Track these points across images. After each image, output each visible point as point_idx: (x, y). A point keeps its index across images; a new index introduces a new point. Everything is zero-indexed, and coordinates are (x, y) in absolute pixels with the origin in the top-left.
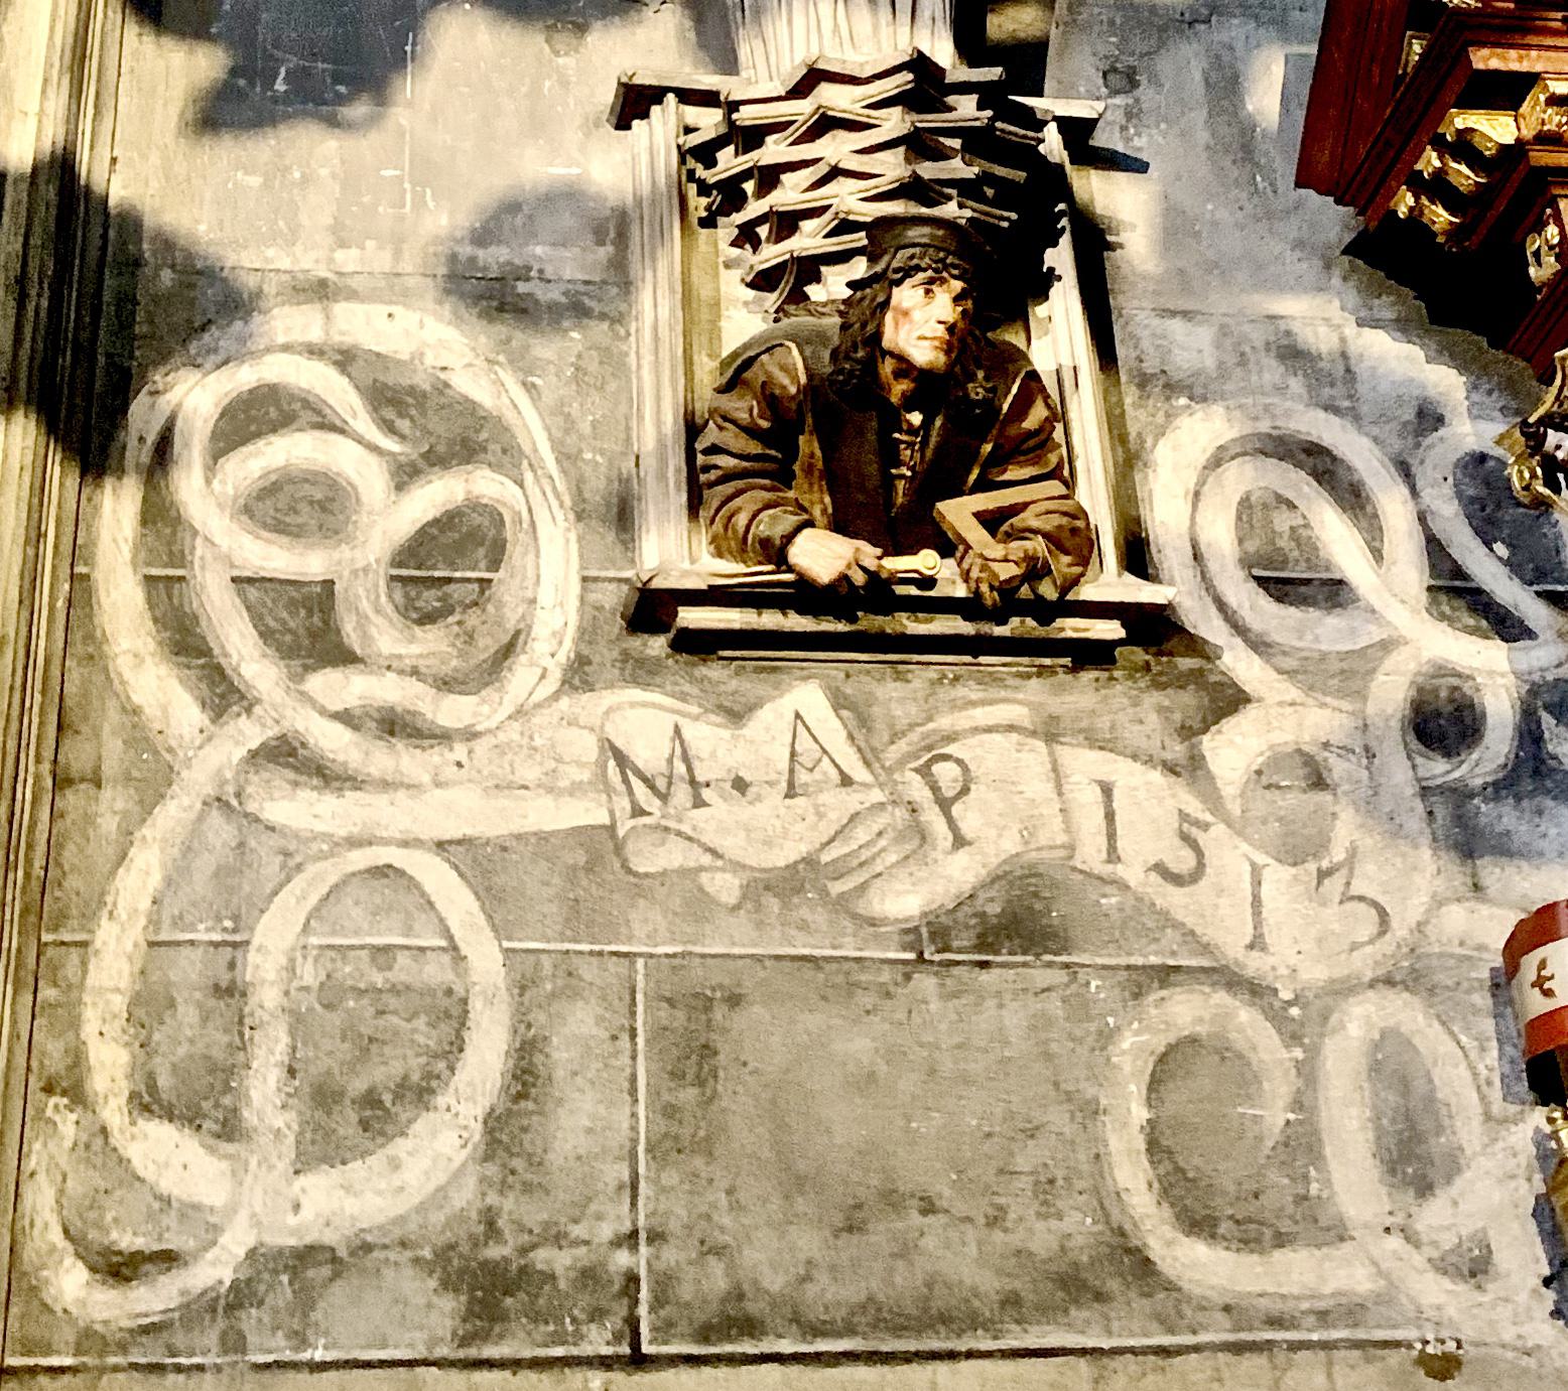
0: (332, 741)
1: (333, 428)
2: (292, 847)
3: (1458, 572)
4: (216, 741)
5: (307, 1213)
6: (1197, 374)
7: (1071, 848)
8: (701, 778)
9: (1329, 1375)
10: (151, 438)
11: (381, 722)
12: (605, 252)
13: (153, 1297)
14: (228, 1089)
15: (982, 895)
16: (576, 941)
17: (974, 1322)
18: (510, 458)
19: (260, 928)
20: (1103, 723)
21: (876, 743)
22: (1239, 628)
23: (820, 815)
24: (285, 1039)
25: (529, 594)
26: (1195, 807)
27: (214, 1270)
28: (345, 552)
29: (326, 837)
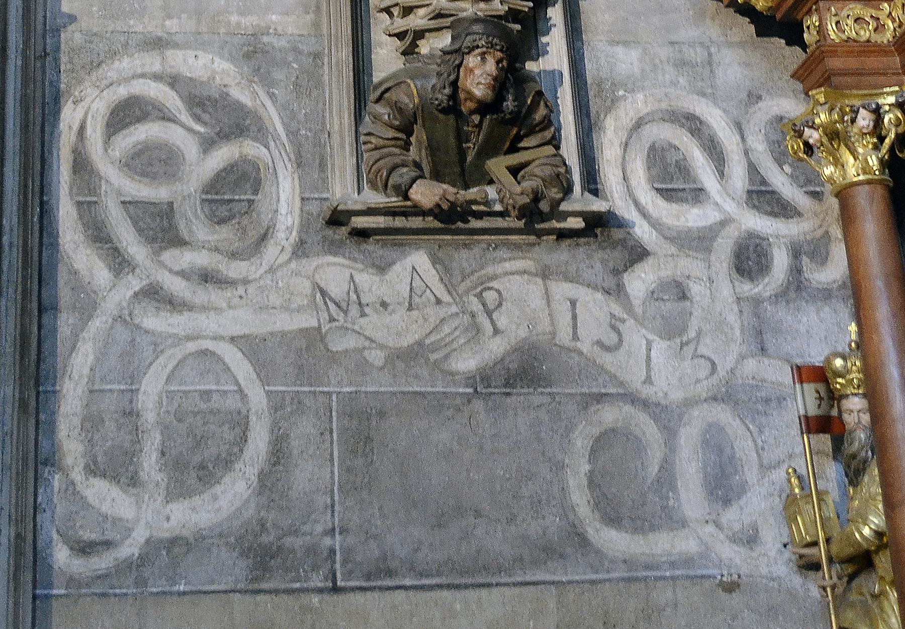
0: (177, 286)
1: (169, 120)
2: (159, 340)
3: (764, 182)
4: (117, 288)
5: (173, 521)
6: (629, 77)
7: (554, 334)
8: (363, 302)
9: (674, 591)
10: (76, 127)
11: (201, 276)
12: (310, 17)
13: (102, 562)
14: (131, 462)
15: (508, 359)
16: (301, 385)
18: (261, 134)
19: (144, 382)
20: (573, 268)
21: (454, 282)
22: (645, 215)
24: (159, 437)
25: (275, 207)
26: (617, 310)
27: (130, 549)
28: (178, 186)
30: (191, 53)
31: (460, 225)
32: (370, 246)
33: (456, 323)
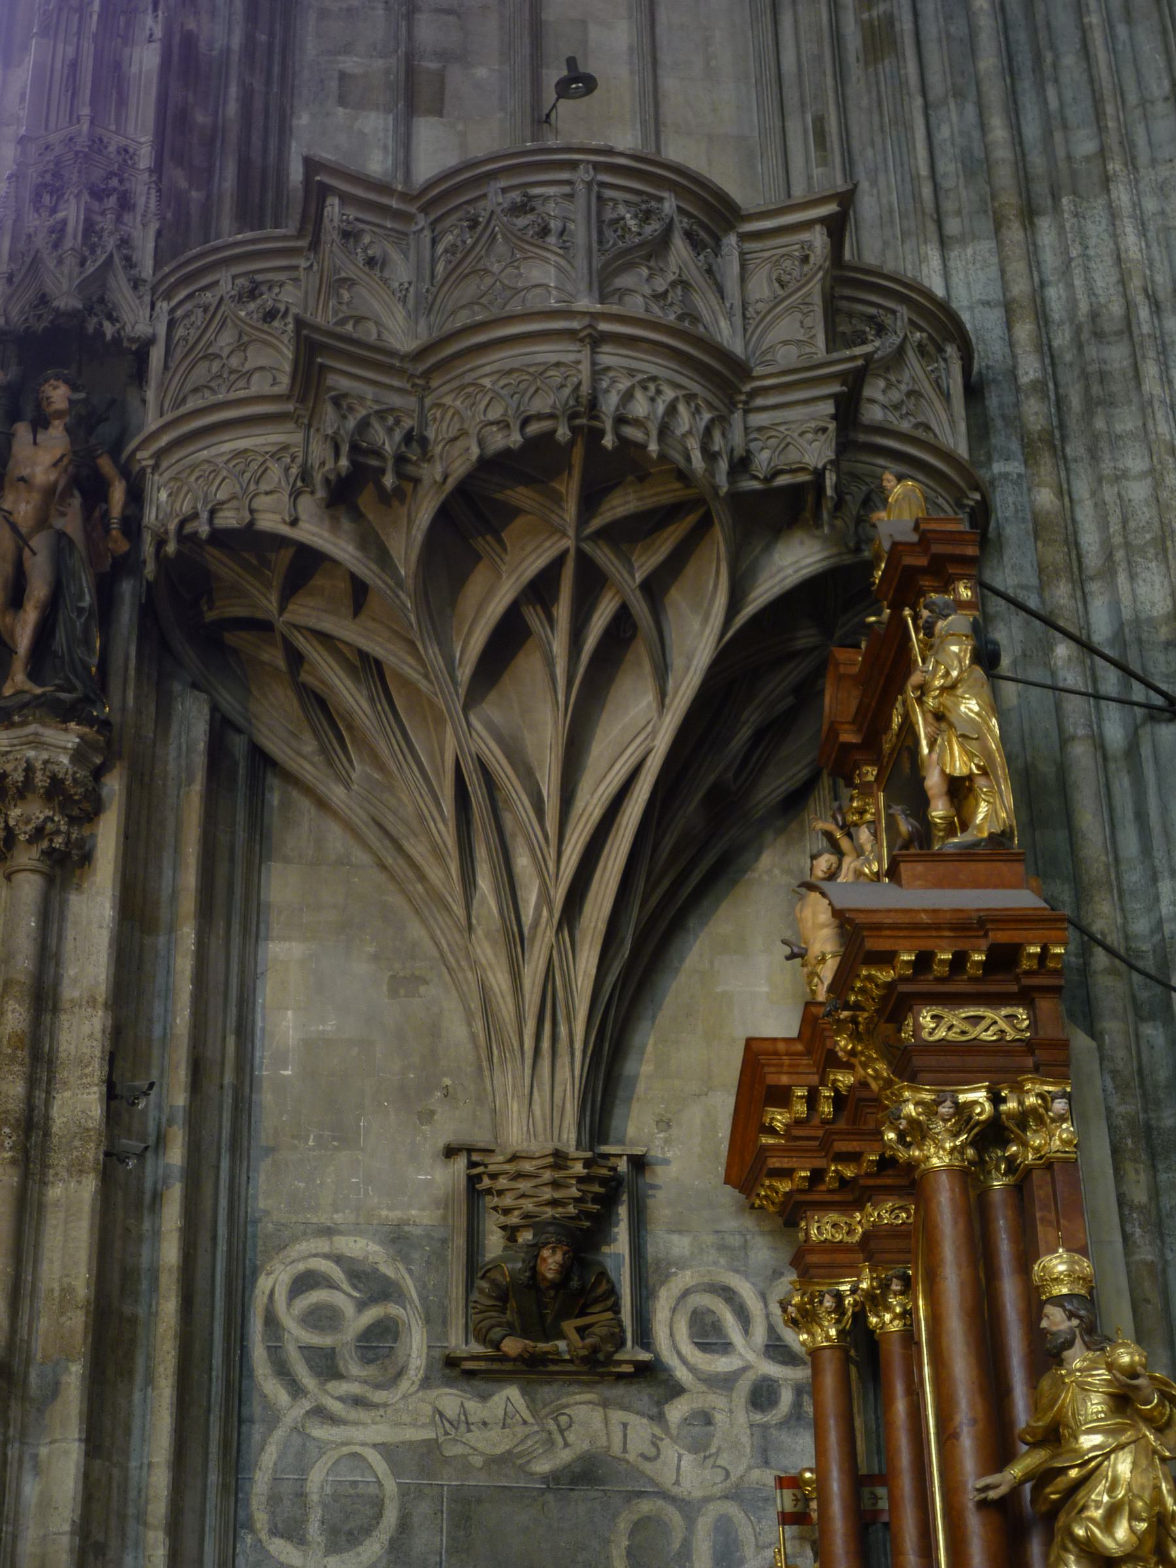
0: (336, 1407)
7: (609, 1448)
10: (267, 1292)
23: (515, 1435)
29: (333, 1442)
30: (353, 1239)
31: (541, 1368)
33: (537, 1438)
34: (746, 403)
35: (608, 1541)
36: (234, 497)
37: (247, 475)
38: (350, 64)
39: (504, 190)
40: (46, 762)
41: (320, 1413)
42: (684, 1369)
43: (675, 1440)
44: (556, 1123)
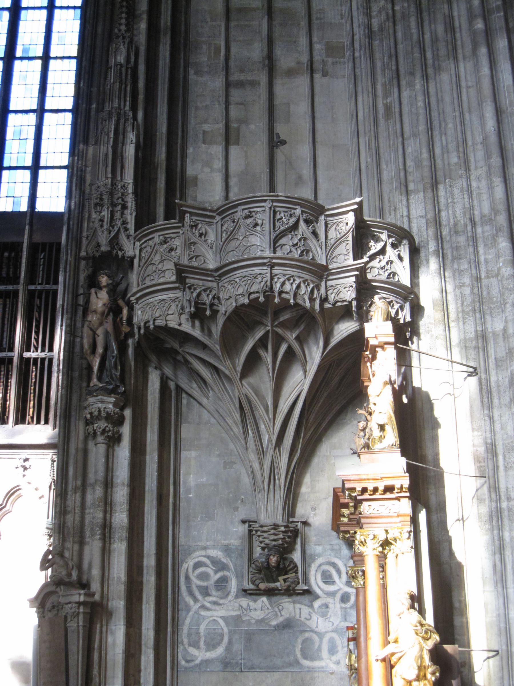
0: (208, 605)
8: (251, 608)
13: (192, 664)
17: (279, 668)
24: (204, 638)
27: (198, 662)
30: (212, 550)
32: (253, 596)
34: (326, 278)
35: (295, 646)
36: (160, 316)
37: (165, 308)
38: (207, 127)
39: (243, 210)
40: (105, 408)
41: (203, 607)
42: (319, 590)
43: (316, 613)
44: (275, 513)
